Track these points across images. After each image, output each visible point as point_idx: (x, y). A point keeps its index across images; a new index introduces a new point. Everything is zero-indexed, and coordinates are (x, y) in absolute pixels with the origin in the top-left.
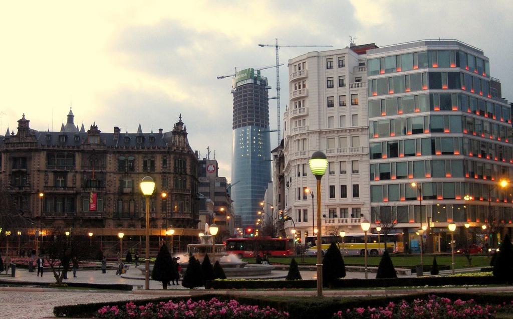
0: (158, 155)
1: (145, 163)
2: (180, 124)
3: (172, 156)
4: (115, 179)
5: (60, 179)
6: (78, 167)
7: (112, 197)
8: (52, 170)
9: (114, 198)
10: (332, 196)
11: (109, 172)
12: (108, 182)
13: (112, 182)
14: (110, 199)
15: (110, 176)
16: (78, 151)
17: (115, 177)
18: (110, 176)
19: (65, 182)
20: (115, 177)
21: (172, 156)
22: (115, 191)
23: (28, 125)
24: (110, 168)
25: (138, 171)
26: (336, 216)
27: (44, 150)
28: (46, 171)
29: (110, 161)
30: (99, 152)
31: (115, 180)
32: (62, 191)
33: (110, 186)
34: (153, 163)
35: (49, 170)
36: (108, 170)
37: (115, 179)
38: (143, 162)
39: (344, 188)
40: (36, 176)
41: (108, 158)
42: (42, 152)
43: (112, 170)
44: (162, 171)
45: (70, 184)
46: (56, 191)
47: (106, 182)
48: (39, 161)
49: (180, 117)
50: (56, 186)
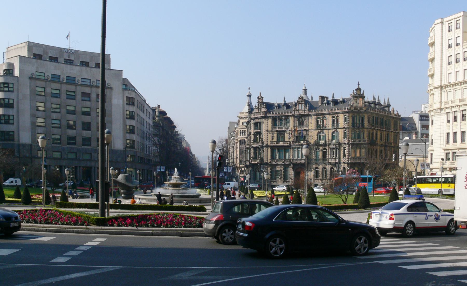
0: (341, 115)
2: (359, 89)
4: (314, 134)
5: (281, 136)
6: (292, 127)
8: (276, 130)
10: (448, 142)
12: (310, 137)
15: (311, 132)
16: (291, 116)
17: (314, 133)
19: (283, 138)
20: (314, 133)
23: (262, 100)
26: (449, 159)
31: (314, 135)
32: (281, 144)
33: (311, 140)
34: (337, 121)
37: (314, 134)
38: (331, 121)
39: (455, 133)
44: (343, 127)
45: (287, 139)
46: (278, 145)
48: (267, 125)
49: (359, 85)
50: (278, 141)
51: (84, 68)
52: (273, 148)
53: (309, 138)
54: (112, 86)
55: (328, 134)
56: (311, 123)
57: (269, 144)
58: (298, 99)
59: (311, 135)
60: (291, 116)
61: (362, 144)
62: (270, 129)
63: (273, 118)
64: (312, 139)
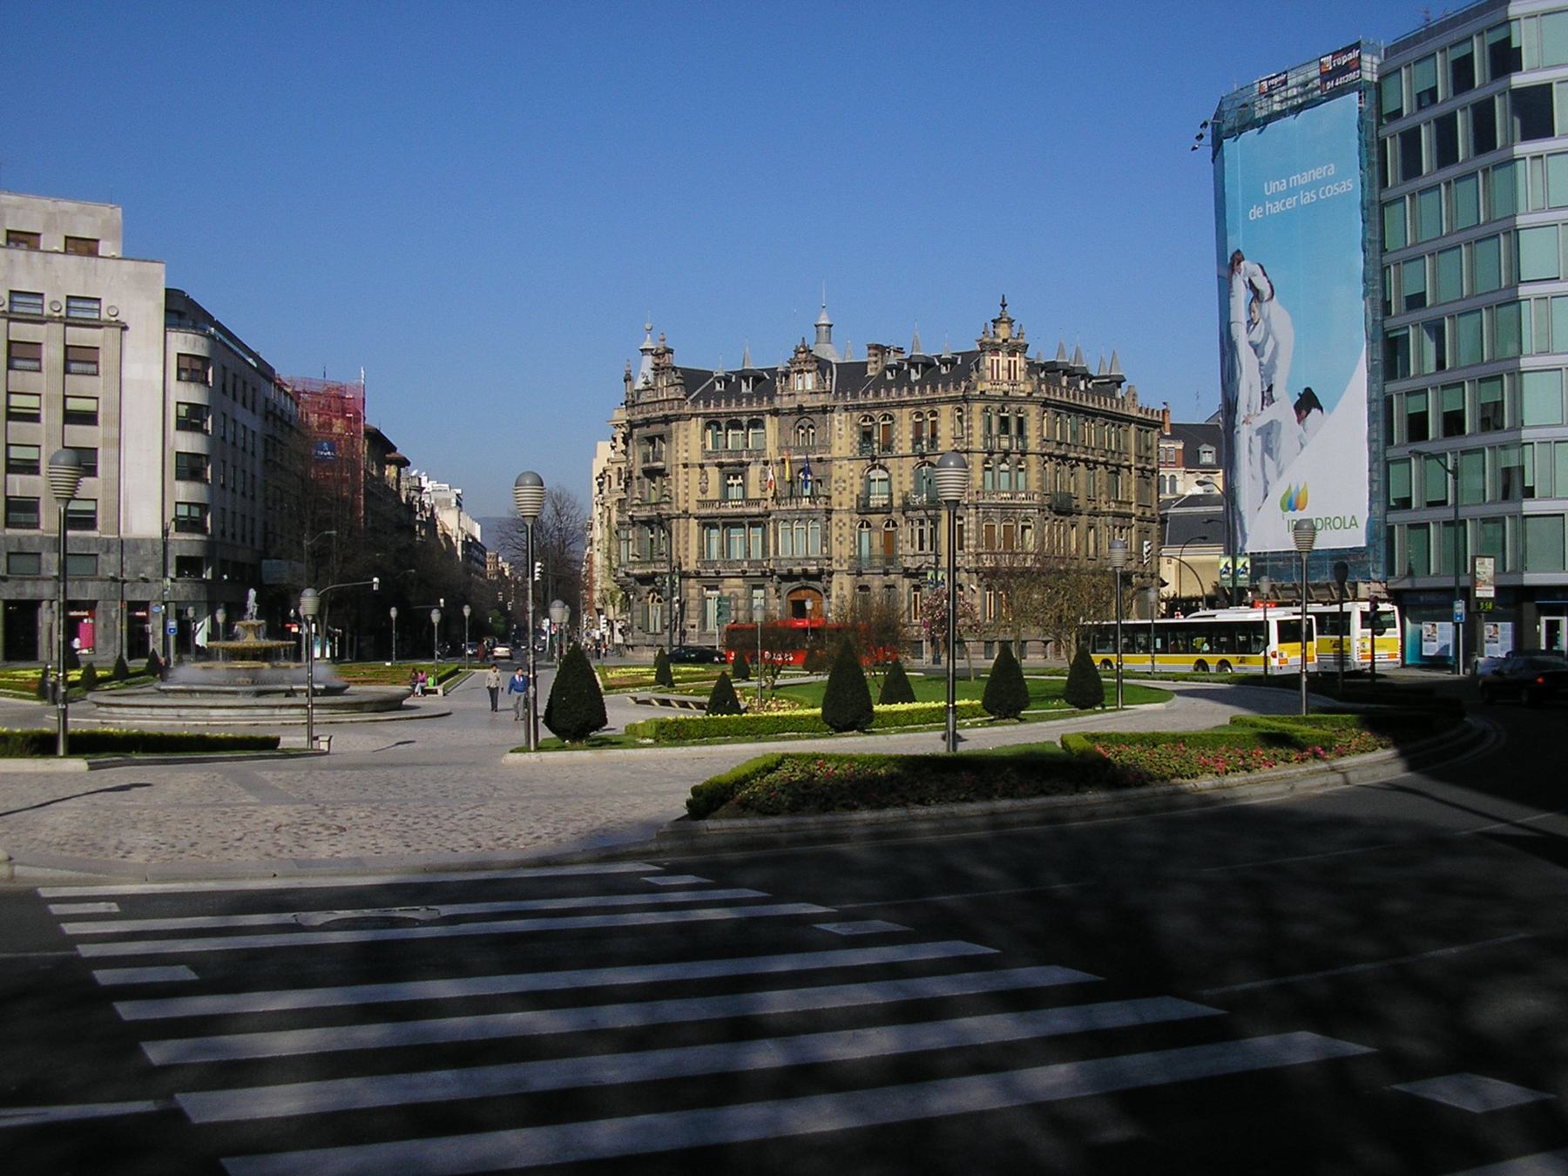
0: (941, 407)
1: (918, 428)
3: (977, 407)
4: (851, 474)
5: (735, 482)
7: (846, 517)
8: (716, 461)
9: (851, 520)
11: (837, 459)
12: (836, 482)
13: (844, 481)
14: (841, 524)
15: (840, 467)
17: (851, 470)
18: (840, 467)
20: (851, 470)
21: (977, 407)
22: (851, 504)
24: (840, 449)
25: (900, 452)
27: (698, 415)
28: (702, 466)
29: (840, 430)
30: (814, 410)
31: (852, 478)
35: (710, 461)
36: (836, 452)
37: (851, 474)
38: (911, 428)
40: (681, 477)
41: (836, 423)
42: (694, 419)
43: (846, 452)
45: (754, 493)
47: (833, 482)
49: (1004, 306)
50: (725, 498)
51: (20, 255)
52: (707, 523)
53: (834, 485)
54: (122, 318)
55: (902, 476)
56: (842, 433)
57: (693, 509)
58: (793, 357)
59: (840, 478)
60: (769, 412)
61: (1021, 506)
62: (696, 457)
63: (708, 420)
64: (844, 489)
